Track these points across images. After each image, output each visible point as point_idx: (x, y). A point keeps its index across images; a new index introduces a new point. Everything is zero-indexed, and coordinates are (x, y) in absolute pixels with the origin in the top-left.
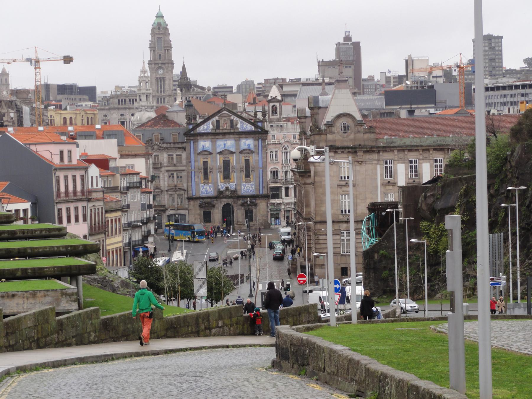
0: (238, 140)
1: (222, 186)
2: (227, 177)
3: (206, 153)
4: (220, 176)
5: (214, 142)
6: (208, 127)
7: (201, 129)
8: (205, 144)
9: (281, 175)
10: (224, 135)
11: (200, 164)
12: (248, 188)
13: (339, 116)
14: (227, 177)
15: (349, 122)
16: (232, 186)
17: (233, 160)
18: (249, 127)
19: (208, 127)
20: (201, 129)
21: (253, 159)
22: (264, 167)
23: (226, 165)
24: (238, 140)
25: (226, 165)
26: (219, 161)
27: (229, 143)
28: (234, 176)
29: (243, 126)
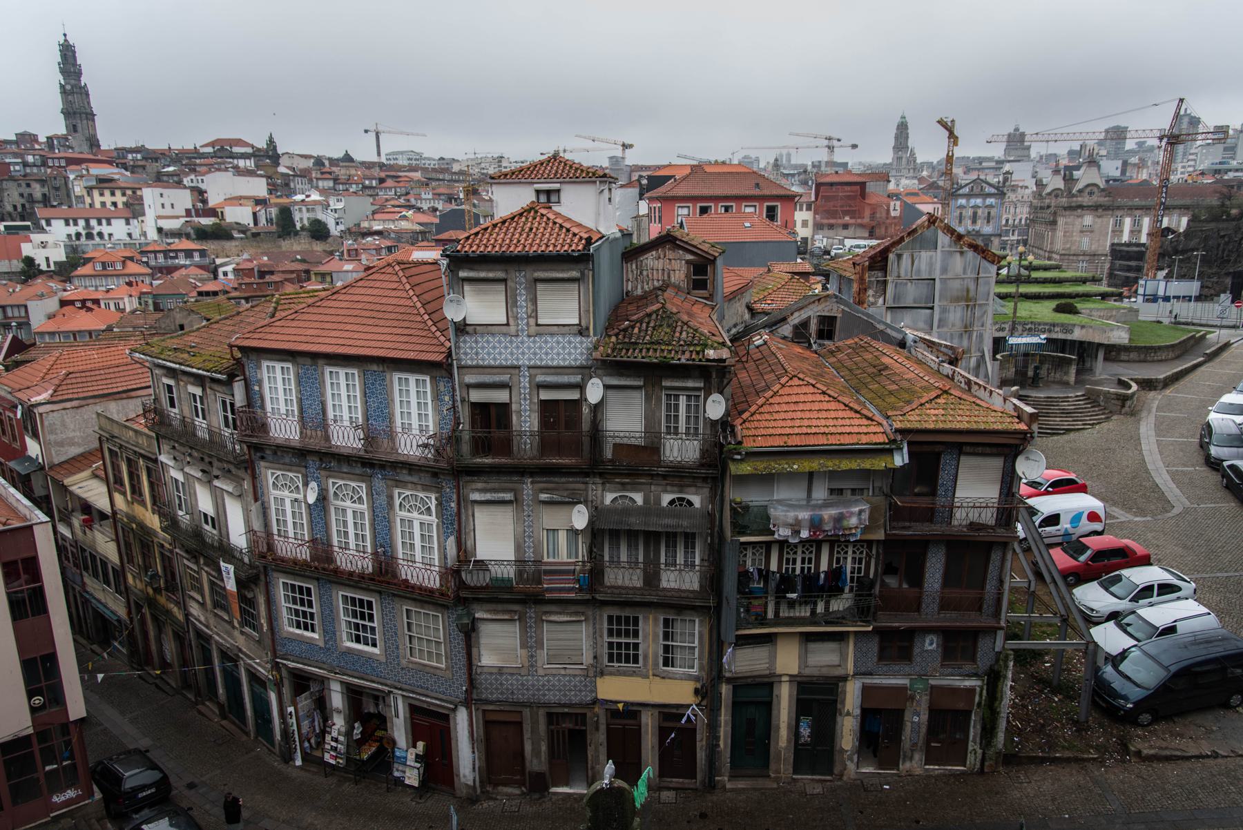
0: (984, 200)
1: (970, 228)
2: (974, 222)
3: (962, 207)
4: (969, 222)
5: (968, 201)
6: (966, 190)
7: (961, 192)
8: (962, 201)
9: (1010, 222)
10: (977, 196)
11: (957, 213)
12: (987, 229)
13: (1088, 185)
14: (974, 222)
15: (1095, 190)
16: (977, 228)
17: (980, 212)
18: (993, 191)
19: (966, 190)
20: (961, 192)
21: (993, 212)
22: (1000, 217)
23: (975, 214)
24: (984, 200)
25: (975, 214)
26: (970, 212)
27: (979, 201)
28: (979, 222)
29: (988, 190)
